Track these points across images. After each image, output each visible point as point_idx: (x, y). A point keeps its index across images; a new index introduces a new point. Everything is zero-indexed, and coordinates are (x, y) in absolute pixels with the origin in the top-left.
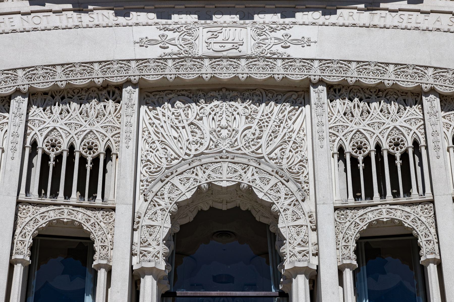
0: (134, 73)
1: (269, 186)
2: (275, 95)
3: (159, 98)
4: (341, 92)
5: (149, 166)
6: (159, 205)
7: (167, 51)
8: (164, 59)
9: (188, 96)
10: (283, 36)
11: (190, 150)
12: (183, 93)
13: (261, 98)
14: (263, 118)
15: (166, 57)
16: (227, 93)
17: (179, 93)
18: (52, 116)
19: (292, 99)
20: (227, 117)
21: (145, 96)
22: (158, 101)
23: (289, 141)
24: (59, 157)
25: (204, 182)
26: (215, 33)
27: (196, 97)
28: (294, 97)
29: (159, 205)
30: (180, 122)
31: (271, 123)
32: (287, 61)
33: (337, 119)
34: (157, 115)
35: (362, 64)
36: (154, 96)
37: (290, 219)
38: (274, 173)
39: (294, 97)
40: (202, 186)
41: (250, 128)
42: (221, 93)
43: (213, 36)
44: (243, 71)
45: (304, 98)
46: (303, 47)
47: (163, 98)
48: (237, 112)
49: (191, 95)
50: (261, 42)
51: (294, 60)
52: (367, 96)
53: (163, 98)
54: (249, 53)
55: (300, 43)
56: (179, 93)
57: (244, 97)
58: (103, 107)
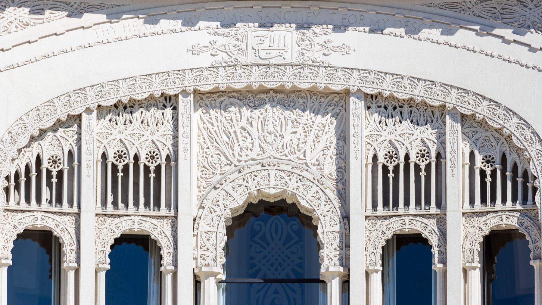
0: (190, 83)
1: (311, 193)
2: (319, 97)
3: (211, 100)
4: (377, 99)
5: (205, 172)
6: (215, 212)
7: (218, 58)
8: (215, 67)
9: (238, 99)
10: (325, 42)
11: (241, 156)
12: (234, 94)
13: (306, 101)
14: (307, 122)
15: (217, 65)
16: (274, 95)
17: (230, 95)
18: (117, 127)
19: (334, 102)
20: (274, 121)
21: (199, 99)
22: (210, 103)
23: (330, 147)
24: (126, 168)
25: (254, 188)
26: (263, 39)
27: (246, 99)
28: (336, 99)
29: (215, 212)
30: (231, 126)
31: (315, 127)
32: (329, 69)
33: (372, 127)
34: (211, 118)
35: (396, 77)
36: (207, 98)
37: (328, 224)
38: (315, 182)
39: (336, 99)
40: (252, 192)
41: (296, 132)
42: (269, 95)
43: (261, 42)
44: (288, 79)
45: (345, 101)
46: (343, 55)
47: (215, 100)
48: (283, 116)
49: (241, 97)
50: (305, 48)
51: (335, 68)
52: (400, 104)
53: (215, 100)
54: (294, 61)
55: (341, 51)
56: (230, 95)
57: (290, 99)
58: (161, 114)
